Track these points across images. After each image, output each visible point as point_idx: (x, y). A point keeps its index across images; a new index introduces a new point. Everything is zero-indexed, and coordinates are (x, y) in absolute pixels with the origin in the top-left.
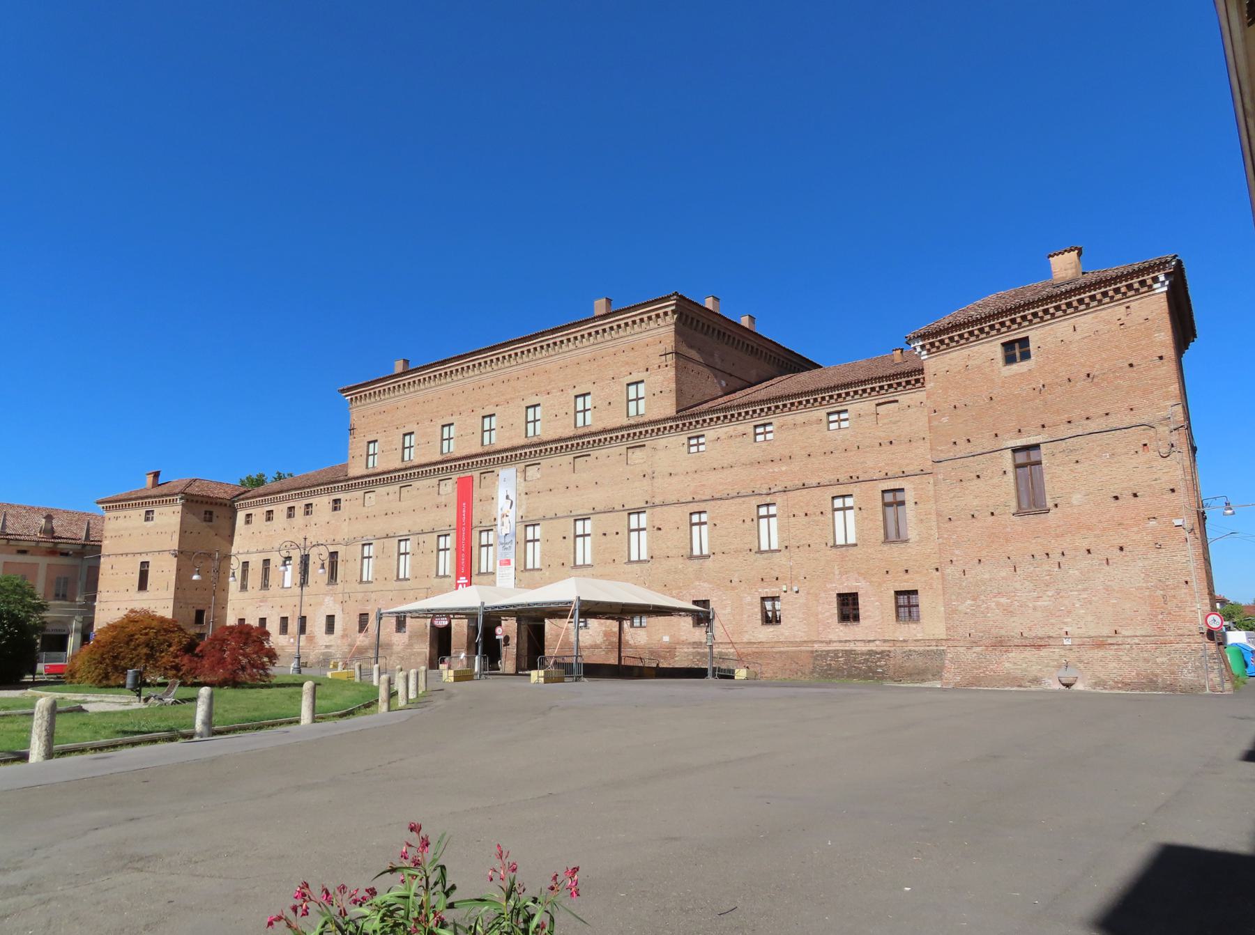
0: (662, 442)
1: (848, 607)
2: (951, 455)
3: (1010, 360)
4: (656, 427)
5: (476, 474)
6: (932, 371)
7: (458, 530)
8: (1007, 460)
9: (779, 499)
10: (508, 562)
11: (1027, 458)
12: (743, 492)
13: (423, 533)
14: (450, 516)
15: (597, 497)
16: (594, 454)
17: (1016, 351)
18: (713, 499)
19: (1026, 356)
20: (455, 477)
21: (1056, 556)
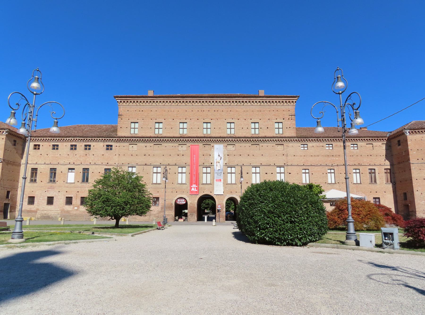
0: (291, 144)
2: (417, 162)
4: (290, 139)
5: (201, 145)
6: (410, 139)
7: (191, 166)
10: (220, 180)
12: (322, 164)
14: (187, 160)
15: (264, 160)
16: (261, 144)
18: (311, 165)
20: (189, 144)
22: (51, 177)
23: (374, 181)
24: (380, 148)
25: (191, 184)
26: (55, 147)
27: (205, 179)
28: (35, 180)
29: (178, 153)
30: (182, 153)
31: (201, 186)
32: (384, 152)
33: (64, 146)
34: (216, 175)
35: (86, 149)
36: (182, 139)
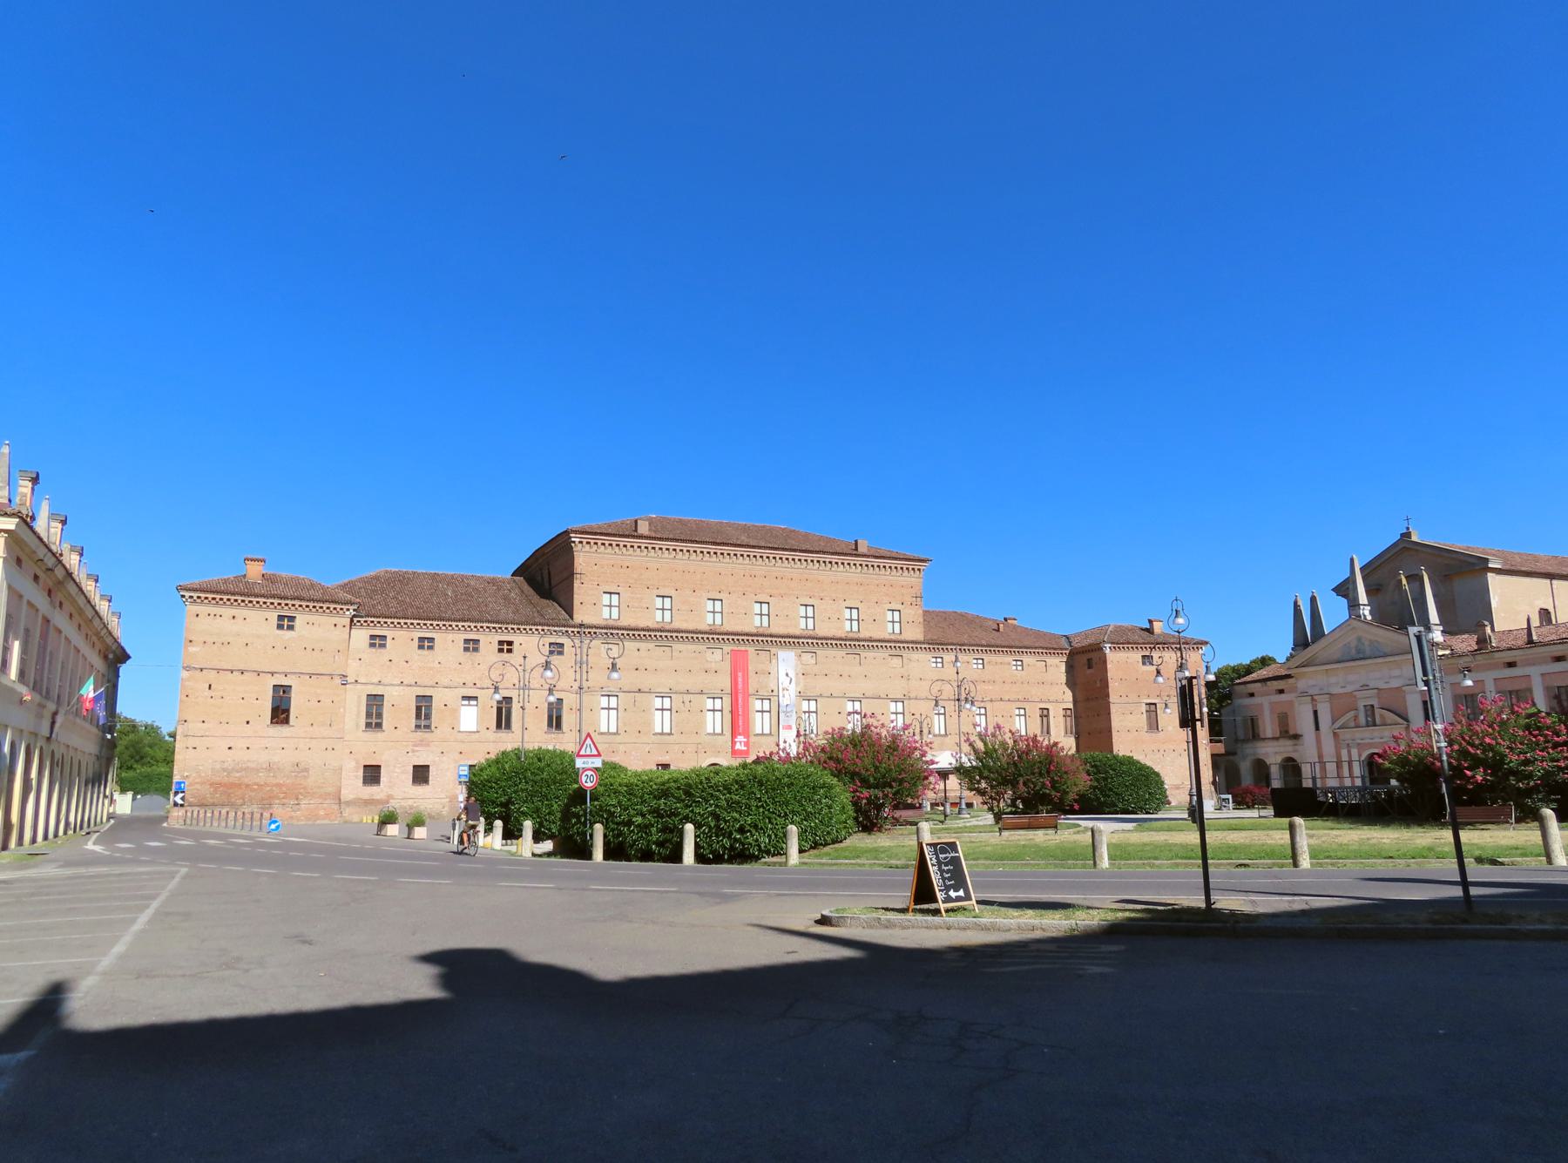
0: (915, 656)
4: (914, 645)
5: (751, 650)
8: (1144, 708)
13: (688, 692)
14: (725, 682)
15: (868, 687)
20: (727, 648)
22: (418, 716)
24: (1057, 667)
25: (734, 735)
26: (426, 643)
28: (379, 725)
29: (707, 666)
30: (714, 666)
31: (753, 739)
32: (1063, 678)
33: (449, 641)
35: (501, 650)
36: (713, 636)
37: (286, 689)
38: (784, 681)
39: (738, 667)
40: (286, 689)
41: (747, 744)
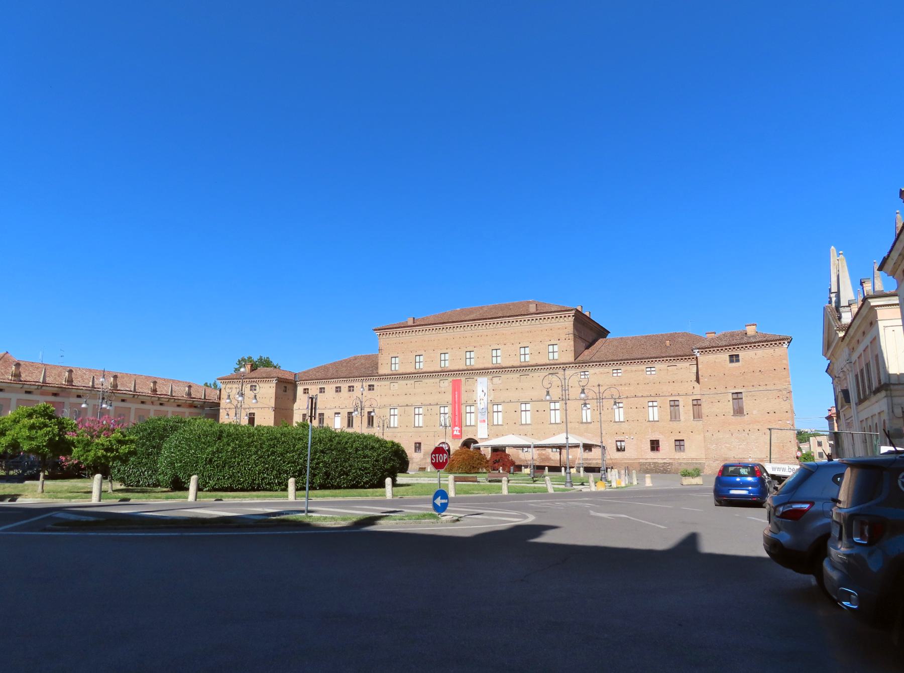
1: (655, 445)
3: (731, 361)
5: (463, 379)
8: (730, 397)
9: (624, 401)
11: (737, 396)
14: (449, 397)
17: (734, 358)
19: (738, 361)
20: (450, 379)
21: (747, 431)
23: (675, 417)
27: (469, 419)
30: (443, 389)
31: (464, 428)
34: (479, 415)
37: (254, 414)
38: (479, 394)
39: (456, 387)
40: (254, 414)
41: (461, 431)
